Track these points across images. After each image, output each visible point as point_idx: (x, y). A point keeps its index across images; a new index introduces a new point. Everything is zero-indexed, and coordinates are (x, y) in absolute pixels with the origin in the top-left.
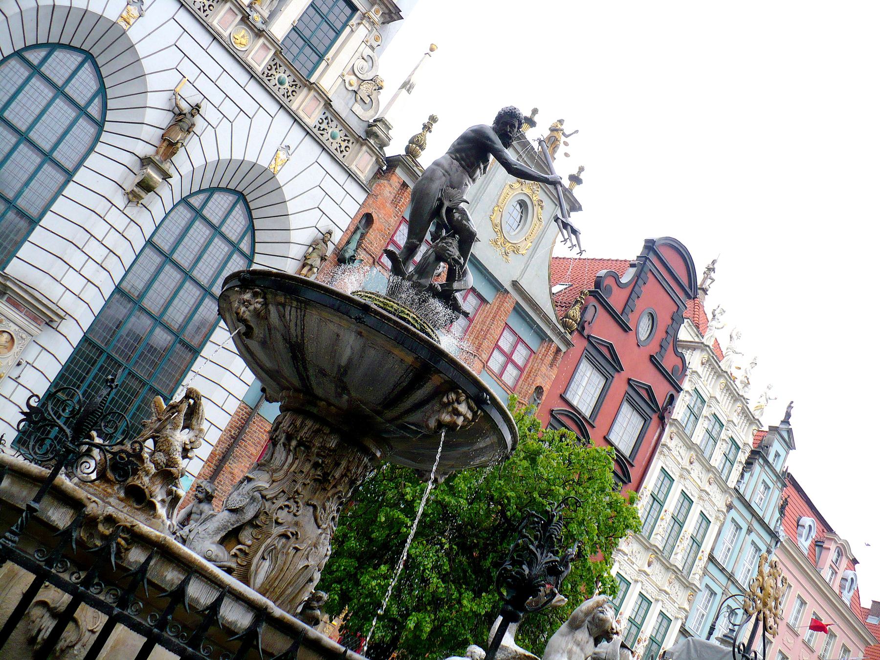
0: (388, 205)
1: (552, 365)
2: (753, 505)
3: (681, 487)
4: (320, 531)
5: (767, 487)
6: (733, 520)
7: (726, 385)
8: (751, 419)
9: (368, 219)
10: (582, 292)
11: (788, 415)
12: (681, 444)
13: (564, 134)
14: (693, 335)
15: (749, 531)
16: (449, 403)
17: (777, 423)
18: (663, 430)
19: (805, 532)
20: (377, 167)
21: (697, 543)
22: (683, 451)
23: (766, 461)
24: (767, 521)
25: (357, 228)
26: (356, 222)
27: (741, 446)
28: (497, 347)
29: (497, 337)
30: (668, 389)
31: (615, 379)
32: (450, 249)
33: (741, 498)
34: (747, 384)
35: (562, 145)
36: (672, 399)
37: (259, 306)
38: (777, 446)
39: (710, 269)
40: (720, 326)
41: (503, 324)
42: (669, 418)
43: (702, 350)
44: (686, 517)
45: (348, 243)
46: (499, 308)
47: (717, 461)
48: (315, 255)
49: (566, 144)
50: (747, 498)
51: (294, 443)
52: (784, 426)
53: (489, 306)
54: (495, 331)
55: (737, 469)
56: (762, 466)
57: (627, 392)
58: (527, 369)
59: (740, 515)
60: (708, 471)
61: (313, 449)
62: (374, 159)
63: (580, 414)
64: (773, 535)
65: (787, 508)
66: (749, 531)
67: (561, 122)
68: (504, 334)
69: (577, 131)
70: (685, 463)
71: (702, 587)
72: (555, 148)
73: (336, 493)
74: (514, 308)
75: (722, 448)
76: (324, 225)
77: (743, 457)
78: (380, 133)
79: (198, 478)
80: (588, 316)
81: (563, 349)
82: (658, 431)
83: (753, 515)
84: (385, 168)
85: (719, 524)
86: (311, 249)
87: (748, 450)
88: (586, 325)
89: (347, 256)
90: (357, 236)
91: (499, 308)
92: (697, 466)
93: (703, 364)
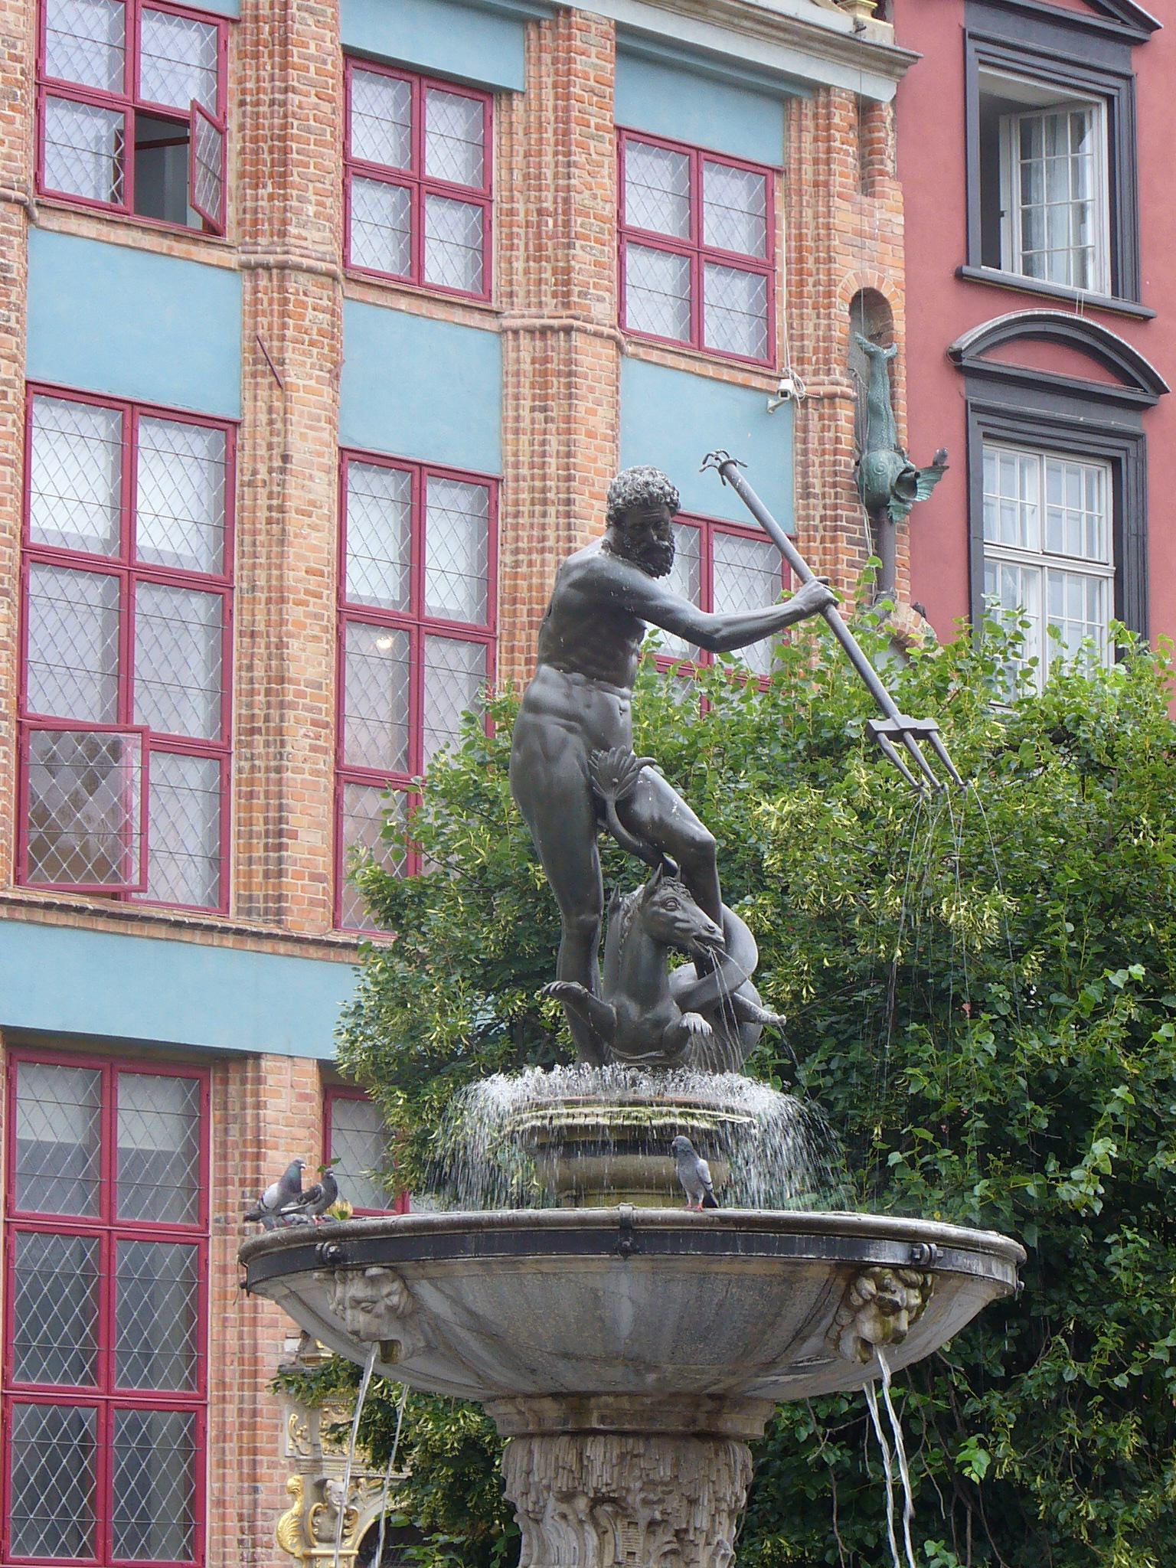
1: (867, 185)
28: (628, 237)
29: (610, 210)
31: (1141, 83)
32: (678, 914)
37: (395, 1299)
41: (607, 145)
46: (564, 94)
53: (518, 103)
54: (592, 191)
58: (782, 252)
61: (630, 1499)
68: (630, 174)
73: (715, 1554)
74: (621, 51)
81: (881, 90)
91: (564, 94)
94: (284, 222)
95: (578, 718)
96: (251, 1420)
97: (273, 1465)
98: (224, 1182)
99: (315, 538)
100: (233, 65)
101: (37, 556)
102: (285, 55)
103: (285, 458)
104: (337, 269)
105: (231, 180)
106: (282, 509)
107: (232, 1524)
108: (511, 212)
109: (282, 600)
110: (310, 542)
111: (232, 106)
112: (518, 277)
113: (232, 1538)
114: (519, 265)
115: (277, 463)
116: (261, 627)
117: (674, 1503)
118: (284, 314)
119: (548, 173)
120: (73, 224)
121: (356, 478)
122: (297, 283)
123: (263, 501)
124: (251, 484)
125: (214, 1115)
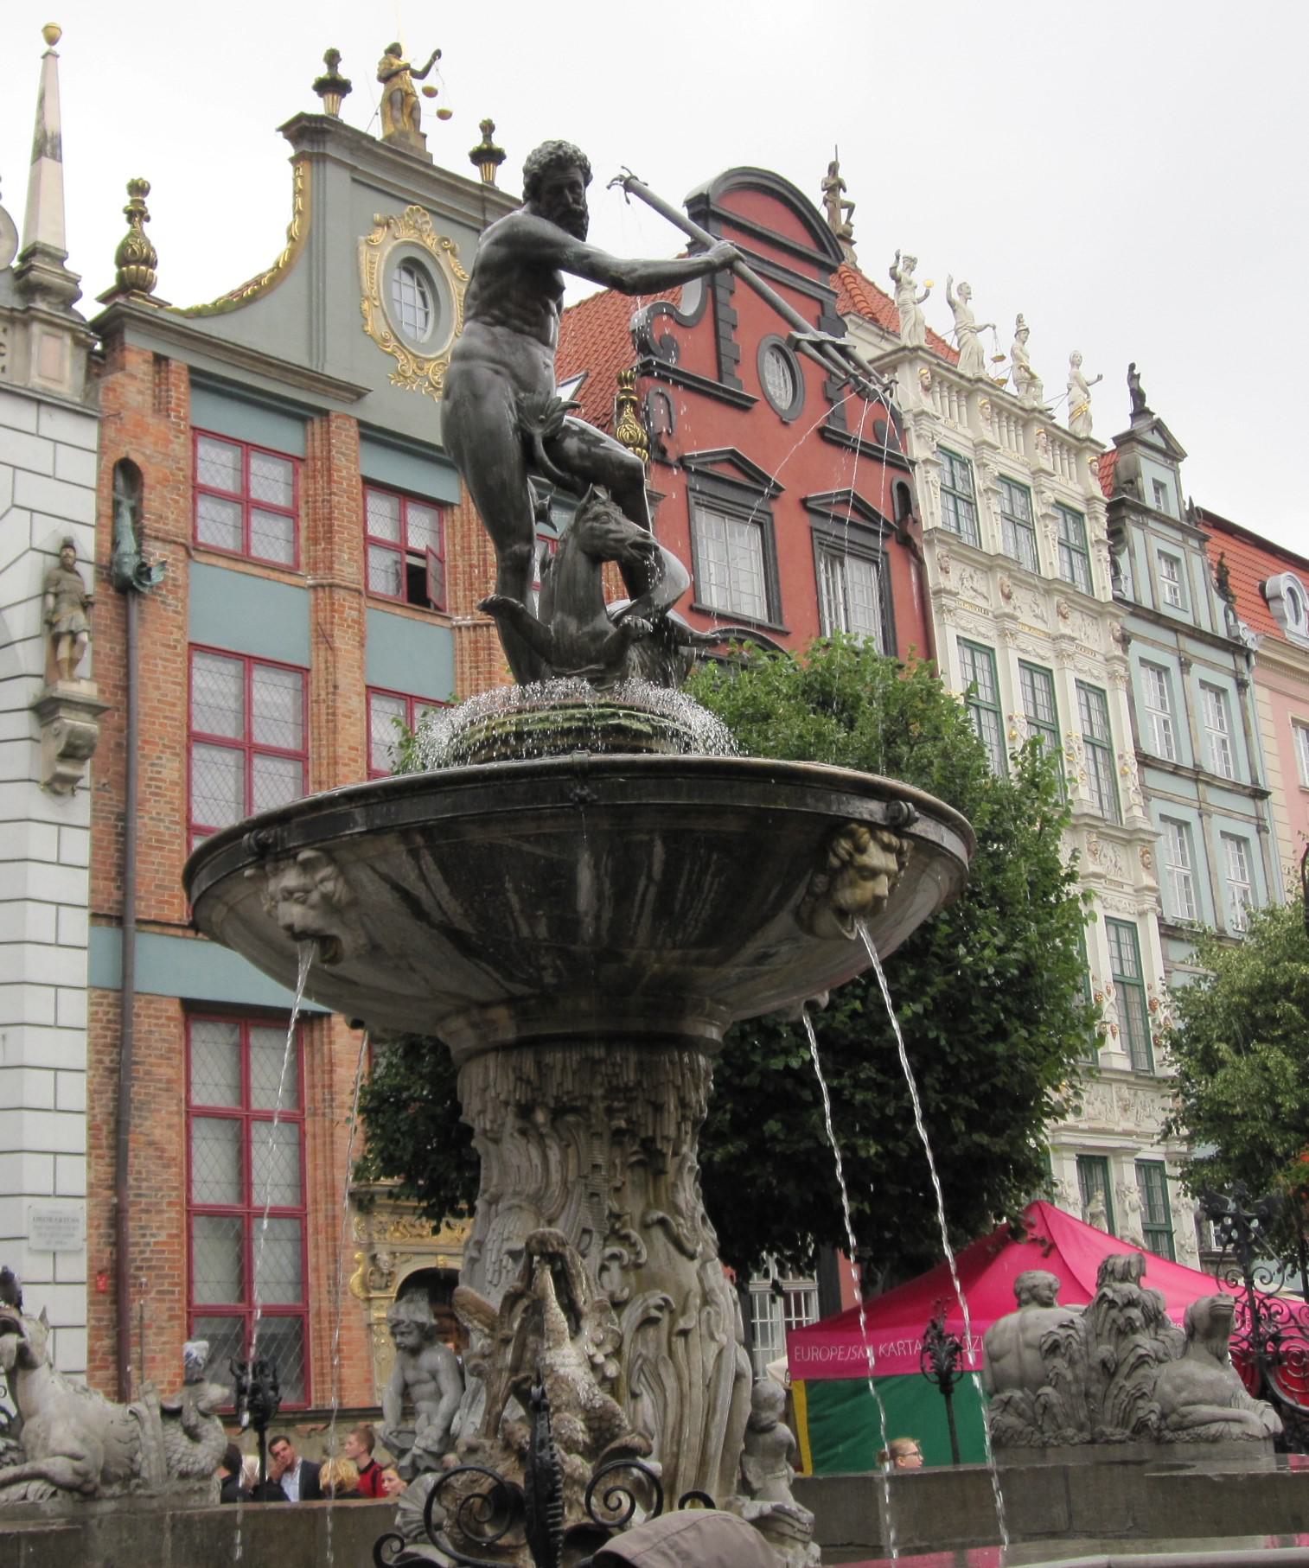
0: (151, 420)
2: (1166, 611)
3: (1014, 656)
4: (697, 1263)
5: (1173, 561)
6: (1144, 662)
7: (993, 405)
8: (1073, 444)
9: (128, 472)
10: (622, 381)
11: (1138, 396)
12: (969, 571)
13: (416, 75)
14: (876, 340)
15: (1185, 666)
16: (847, 864)
17: (1124, 425)
18: (920, 563)
19: (1287, 606)
20: (83, 354)
21: (1100, 747)
22: (980, 583)
23: (1146, 512)
24: (1206, 626)
25: (116, 504)
26: (107, 491)
27: (1081, 508)
30: (884, 475)
31: (777, 518)
32: (612, 526)
33: (1137, 610)
34: (1031, 380)
35: (424, 101)
36: (904, 494)
37: (329, 886)
38: (1150, 470)
39: (834, 187)
40: (920, 293)
42: (920, 533)
43: (911, 362)
44: (1053, 708)
45: (115, 544)
47: (1053, 563)
48: (65, 607)
49: (430, 93)
50: (1147, 603)
51: (540, 1117)
52: (1142, 424)
53: (456, 510)
55: (1100, 558)
56: (1142, 526)
57: (812, 529)
59: (1154, 646)
60: (1048, 593)
61: (593, 1109)
62: (68, 341)
63: (748, 623)
64: (1234, 647)
65: (1230, 581)
66: (1185, 666)
67: (395, 50)
69: (438, 54)
70: (997, 603)
71: (1156, 825)
72: (413, 113)
75: (1049, 534)
76: (47, 534)
77: (1097, 529)
78: (47, 279)
79: (91, 1195)
80: (660, 424)
82: (913, 570)
83: (1176, 631)
84: (98, 347)
85: (1122, 686)
86: (51, 600)
87: (1101, 509)
88: (665, 441)
89: (129, 571)
90: (127, 519)
92: (1020, 596)
93: (927, 389)
94: (332, 562)
95: (506, 365)
96: (333, 1220)
97: (347, 1247)
98: (313, 1086)
99: (353, 730)
100: (302, 483)
101: (195, 738)
102: (330, 476)
103: (335, 687)
104: (362, 588)
105: (302, 541)
106: (334, 714)
107: (324, 1282)
108: (456, 567)
109: (336, 763)
110: (351, 733)
111: (302, 503)
112: (460, 600)
113: (324, 1290)
114: (460, 594)
115: (331, 690)
116: (324, 778)
117: (639, 1110)
118: (333, 611)
119: (474, 545)
120: (214, 560)
121: (376, 703)
122: (339, 595)
123: (324, 711)
124: (317, 702)
125: (306, 1050)
